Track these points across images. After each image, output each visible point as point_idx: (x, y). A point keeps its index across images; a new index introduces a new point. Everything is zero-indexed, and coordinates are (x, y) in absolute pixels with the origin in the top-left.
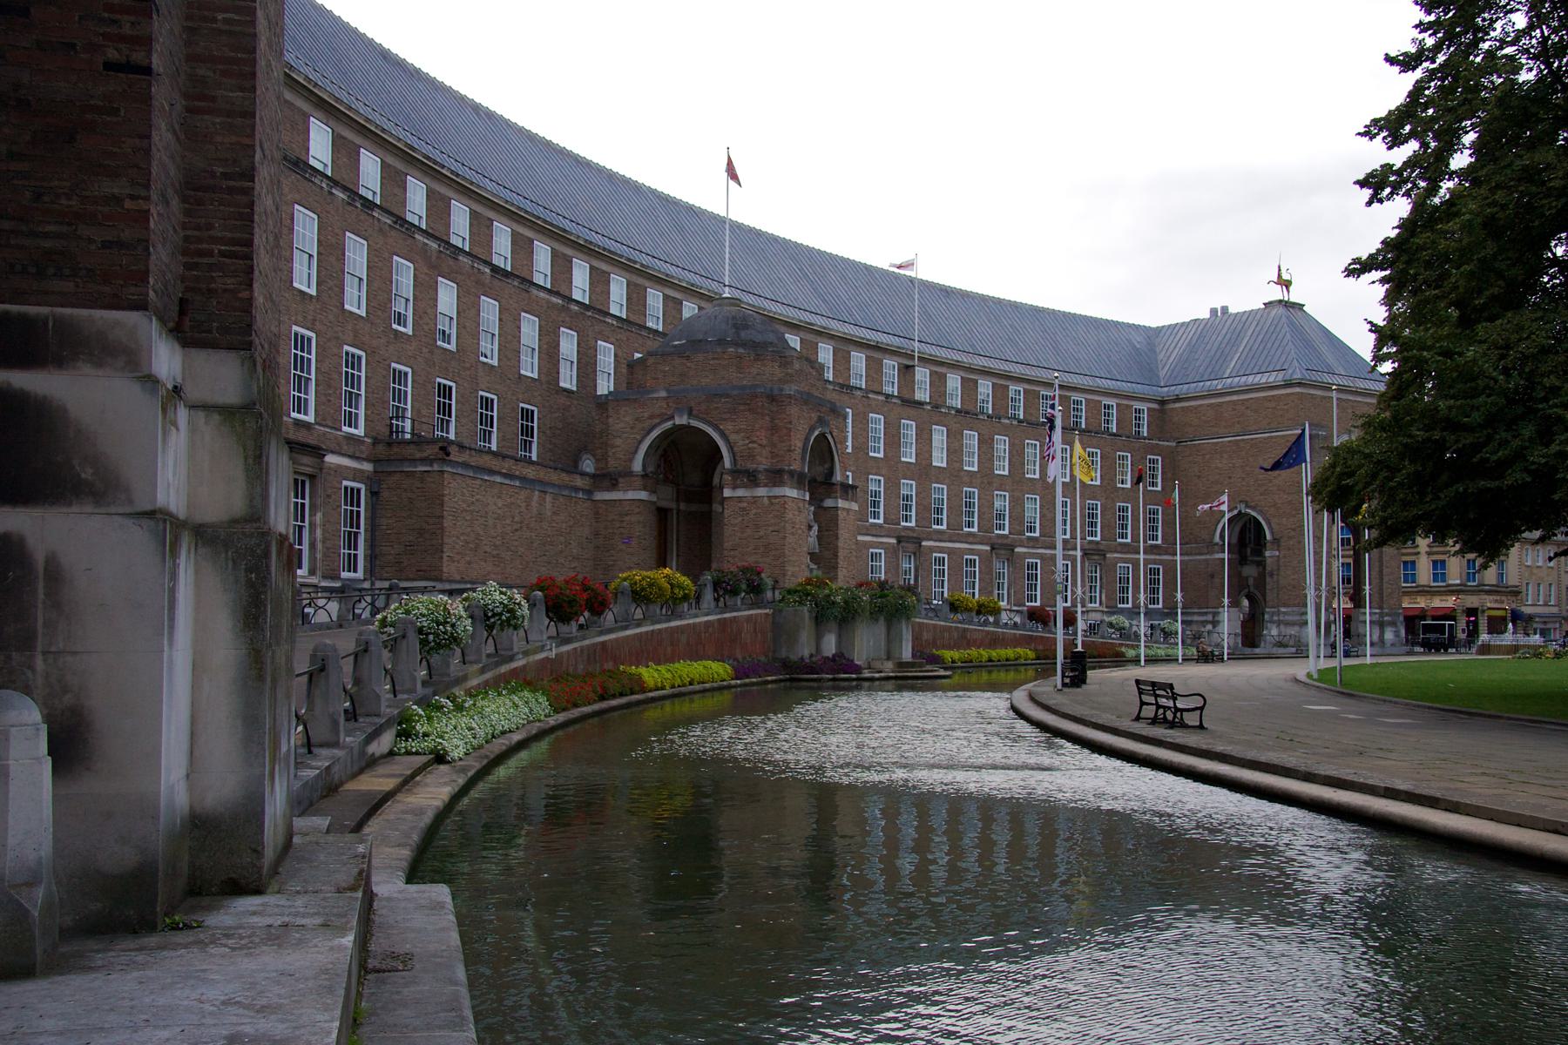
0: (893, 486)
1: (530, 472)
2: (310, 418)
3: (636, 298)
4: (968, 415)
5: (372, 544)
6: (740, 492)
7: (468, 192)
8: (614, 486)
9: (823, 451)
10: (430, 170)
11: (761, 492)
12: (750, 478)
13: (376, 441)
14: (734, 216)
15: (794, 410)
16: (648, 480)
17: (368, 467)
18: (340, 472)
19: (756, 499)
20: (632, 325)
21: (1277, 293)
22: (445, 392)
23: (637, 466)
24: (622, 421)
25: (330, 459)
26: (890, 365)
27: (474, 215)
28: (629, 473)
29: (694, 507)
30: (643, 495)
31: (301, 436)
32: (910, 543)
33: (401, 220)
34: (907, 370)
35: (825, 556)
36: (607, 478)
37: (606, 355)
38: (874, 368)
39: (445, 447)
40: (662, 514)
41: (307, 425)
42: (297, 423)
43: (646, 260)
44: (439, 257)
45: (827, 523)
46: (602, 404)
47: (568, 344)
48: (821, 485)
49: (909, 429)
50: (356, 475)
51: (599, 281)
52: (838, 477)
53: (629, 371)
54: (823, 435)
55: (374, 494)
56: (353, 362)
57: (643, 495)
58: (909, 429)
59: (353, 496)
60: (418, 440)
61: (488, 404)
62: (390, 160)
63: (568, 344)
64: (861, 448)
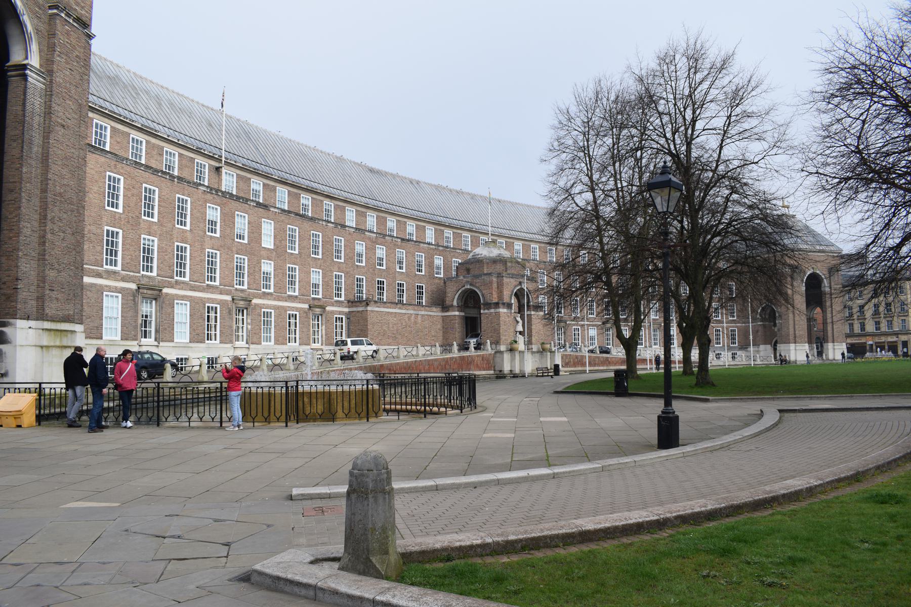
2: (320, 296)
6: (486, 311)
11: (492, 311)
13: (349, 301)
16: (461, 308)
18: (333, 312)
23: (455, 303)
25: (327, 308)
28: (452, 306)
30: (457, 313)
31: (316, 303)
41: (319, 299)
42: (314, 299)
43: (477, 227)
50: (340, 313)
61: (401, 285)
62: (359, 209)
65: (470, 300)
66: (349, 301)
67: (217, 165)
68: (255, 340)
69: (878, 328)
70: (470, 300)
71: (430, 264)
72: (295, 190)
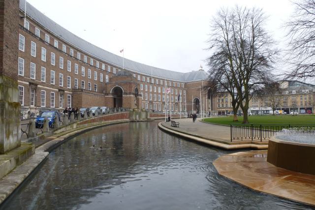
0: (149, 95)
1: (95, 93)
3: (112, 69)
4: (159, 85)
5: (72, 104)
7: (86, 54)
8: (108, 94)
9: (137, 90)
10: (81, 51)
11: (128, 96)
12: (126, 94)
13: (73, 89)
14: (125, 57)
15: (132, 85)
16: (112, 94)
17: (71, 93)
18: (67, 93)
19: (127, 97)
20: (111, 73)
21: (201, 69)
22: (83, 82)
23: (111, 92)
24: (109, 86)
26: (148, 79)
27: (88, 58)
28: (110, 93)
29: (119, 98)
30: (112, 96)
31: (61, 88)
32: (151, 103)
33: (76, 59)
34: (150, 79)
35: (137, 105)
36: (107, 94)
37: (107, 77)
38: (146, 79)
39: (82, 90)
40: (115, 99)
44: (82, 63)
45: (138, 100)
46: (106, 84)
47: (102, 75)
48: (137, 94)
49: (151, 87)
50: (70, 94)
51: (106, 67)
52: (139, 93)
53: (110, 79)
54: (136, 88)
55: (72, 96)
56: (69, 78)
57: (112, 96)
58: (151, 87)
59: (69, 97)
60: (78, 89)
63: (102, 75)
64: (144, 89)
65: (118, 92)
66: (73, 89)
67: (22, 16)
68: (38, 105)
69: (219, 106)
70: (118, 92)
71: (99, 77)
72: (53, 37)
